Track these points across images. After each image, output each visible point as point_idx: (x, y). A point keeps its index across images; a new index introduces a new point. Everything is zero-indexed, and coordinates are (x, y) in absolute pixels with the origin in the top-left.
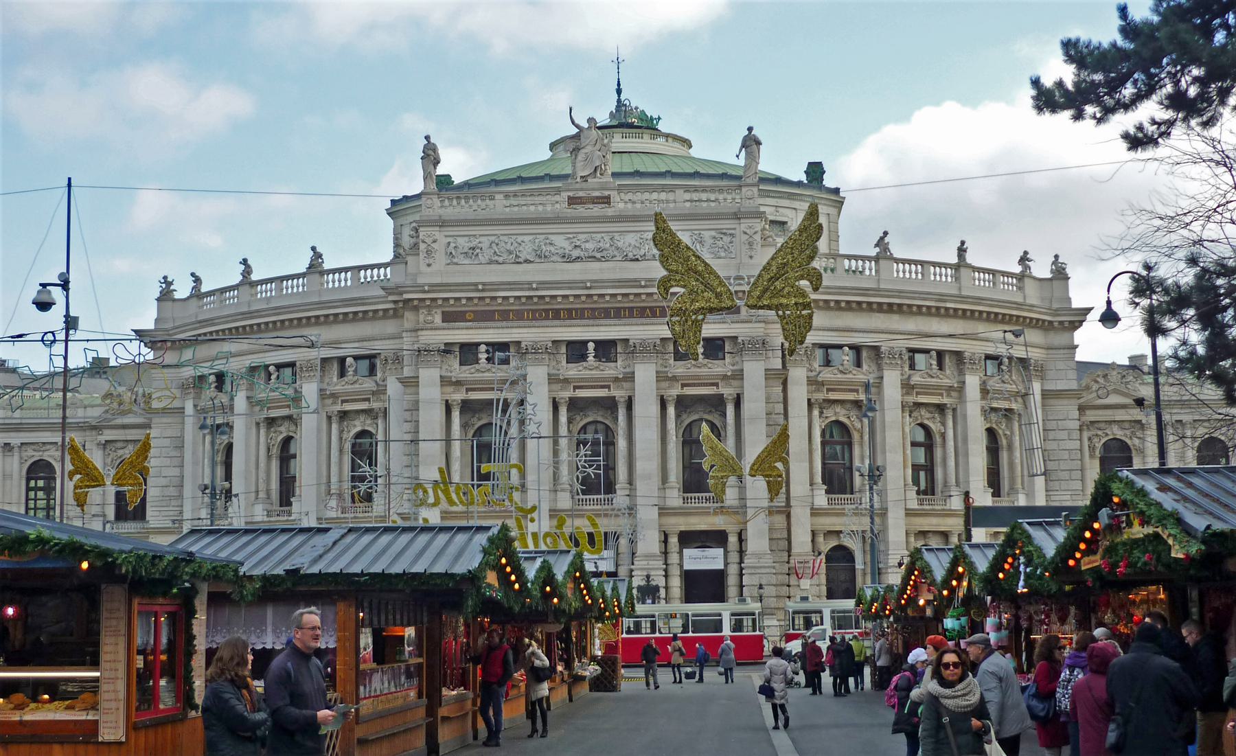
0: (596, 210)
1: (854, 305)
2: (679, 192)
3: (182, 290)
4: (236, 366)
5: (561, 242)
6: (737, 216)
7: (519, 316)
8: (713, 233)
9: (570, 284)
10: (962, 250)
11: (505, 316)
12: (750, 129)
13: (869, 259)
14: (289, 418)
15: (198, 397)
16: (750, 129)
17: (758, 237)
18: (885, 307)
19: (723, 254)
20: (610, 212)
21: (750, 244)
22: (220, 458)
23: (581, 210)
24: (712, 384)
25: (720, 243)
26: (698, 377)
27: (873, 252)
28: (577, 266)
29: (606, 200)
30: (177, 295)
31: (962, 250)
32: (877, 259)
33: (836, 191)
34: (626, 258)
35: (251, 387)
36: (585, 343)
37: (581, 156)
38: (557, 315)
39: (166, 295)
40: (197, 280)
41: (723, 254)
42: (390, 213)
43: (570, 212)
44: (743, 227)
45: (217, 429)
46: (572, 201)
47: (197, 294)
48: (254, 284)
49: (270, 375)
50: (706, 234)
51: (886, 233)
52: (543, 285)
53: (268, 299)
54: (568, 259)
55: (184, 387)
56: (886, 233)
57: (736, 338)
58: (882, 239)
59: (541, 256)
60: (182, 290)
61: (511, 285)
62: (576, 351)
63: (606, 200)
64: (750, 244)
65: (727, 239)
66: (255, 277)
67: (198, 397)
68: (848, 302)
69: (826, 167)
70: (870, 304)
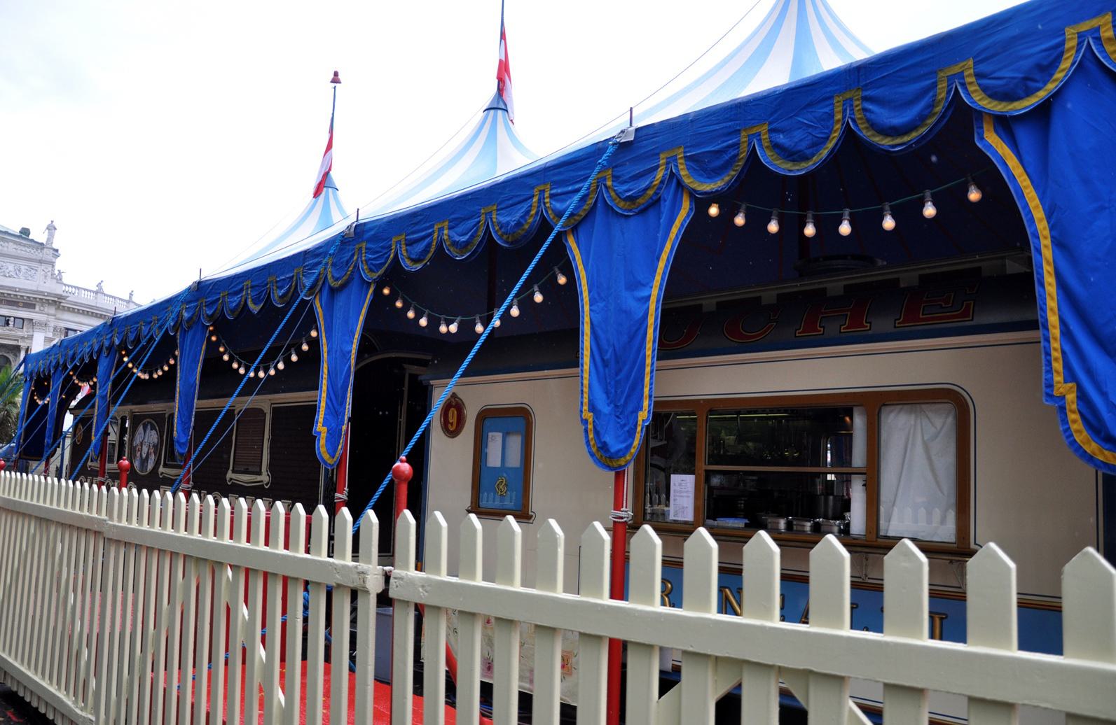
1: (86, 313)
2: (11, 244)
6: (41, 262)
8: (26, 267)
10: (131, 295)
12: (52, 222)
13: (93, 292)
16: (52, 222)
17: (49, 274)
18: (71, 309)
19: (30, 279)
21: (46, 276)
24: (15, 340)
25: (29, 273)
26: (8, 335)
27: (95, 289)
31: (131, 295)
32: (96, 293)
33: (57, 251)
41: (30, 279)
44: (43, 268)
50: (23, 267)
51: (102, 281)
56: (102, 281)
57: (32, 320)
58: (100, 284)
64: (46, 276)
65: (33, 272)
68: (83, 311)
69: (31, 231)
70: (92, 313)
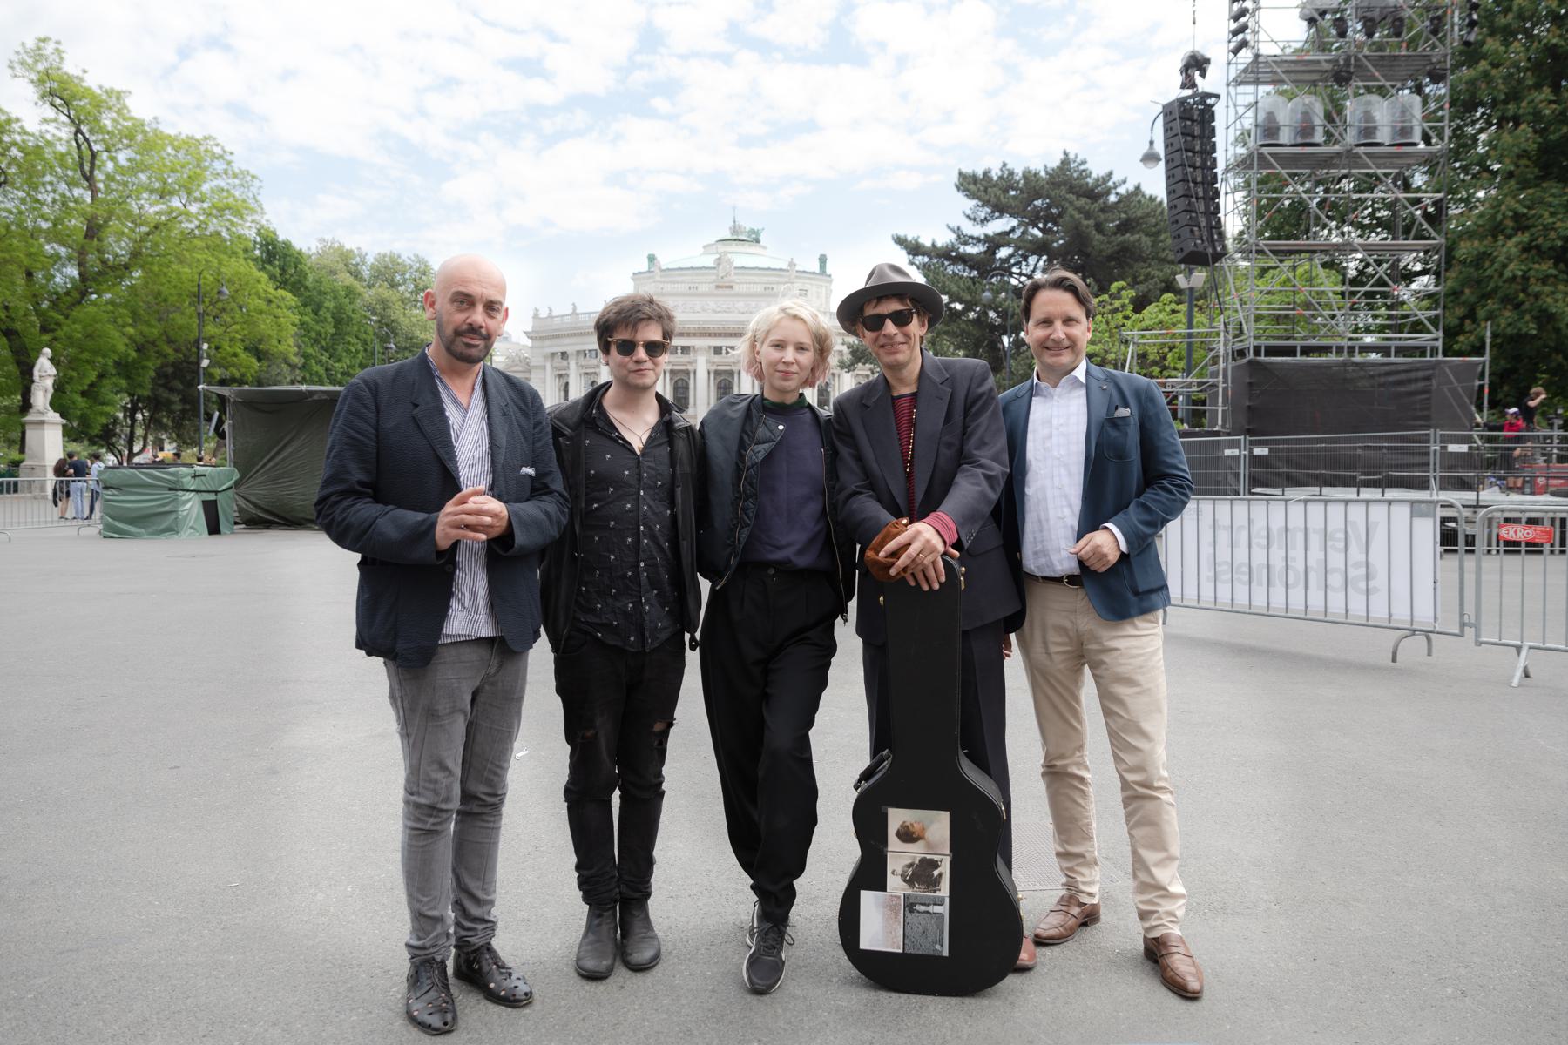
0: (727, 291)
3: (544, 314)
4: (570, 349)
5: (712, 305)
7: (694, 335)
9: (717, 322)
11: (688, 335)
14: (595, 373)
15: (552, 360)
20: (732, 292)
22: (562, 388)
23: (720, 291)
28: (719, 315)
29: (731, 287)
30: (541, 316)
33: (830, 276)
34: (739, 312)
35: (577, 359)
36: (721, 347)
37: (721, 267)
38: (710, 335)
39: (536, 316)
40: (550, 310)
42: (633, 279)
43: (717, 292)
45: (560, 376)
46: (718, 287)
47: (550, 317)
48: (578, 314)
49: (585, 355)
52: (705, 322)
53: (585, 322)
54: (715, 311)
55: (545, 357)
59: (704, 310)
60: (544, 314)
61: (691, 322)
62: (718, 350)
63: (731, 287)
66: (578, 311)
67: (552, 360)
